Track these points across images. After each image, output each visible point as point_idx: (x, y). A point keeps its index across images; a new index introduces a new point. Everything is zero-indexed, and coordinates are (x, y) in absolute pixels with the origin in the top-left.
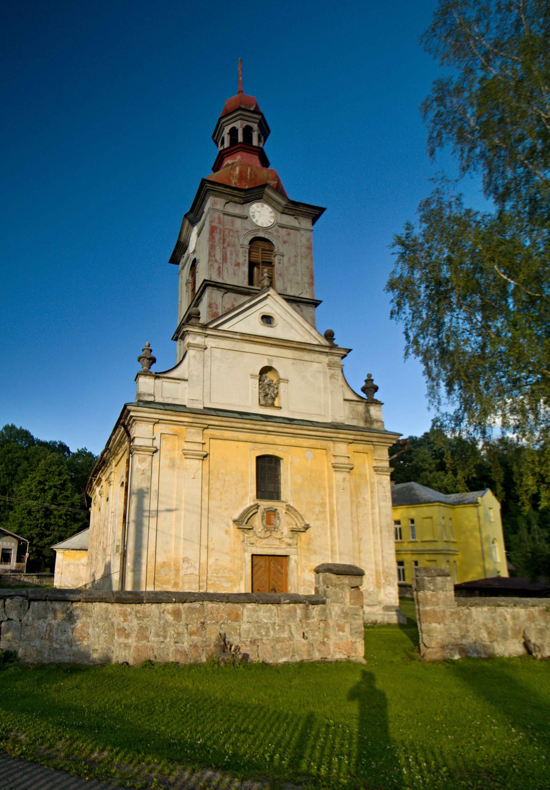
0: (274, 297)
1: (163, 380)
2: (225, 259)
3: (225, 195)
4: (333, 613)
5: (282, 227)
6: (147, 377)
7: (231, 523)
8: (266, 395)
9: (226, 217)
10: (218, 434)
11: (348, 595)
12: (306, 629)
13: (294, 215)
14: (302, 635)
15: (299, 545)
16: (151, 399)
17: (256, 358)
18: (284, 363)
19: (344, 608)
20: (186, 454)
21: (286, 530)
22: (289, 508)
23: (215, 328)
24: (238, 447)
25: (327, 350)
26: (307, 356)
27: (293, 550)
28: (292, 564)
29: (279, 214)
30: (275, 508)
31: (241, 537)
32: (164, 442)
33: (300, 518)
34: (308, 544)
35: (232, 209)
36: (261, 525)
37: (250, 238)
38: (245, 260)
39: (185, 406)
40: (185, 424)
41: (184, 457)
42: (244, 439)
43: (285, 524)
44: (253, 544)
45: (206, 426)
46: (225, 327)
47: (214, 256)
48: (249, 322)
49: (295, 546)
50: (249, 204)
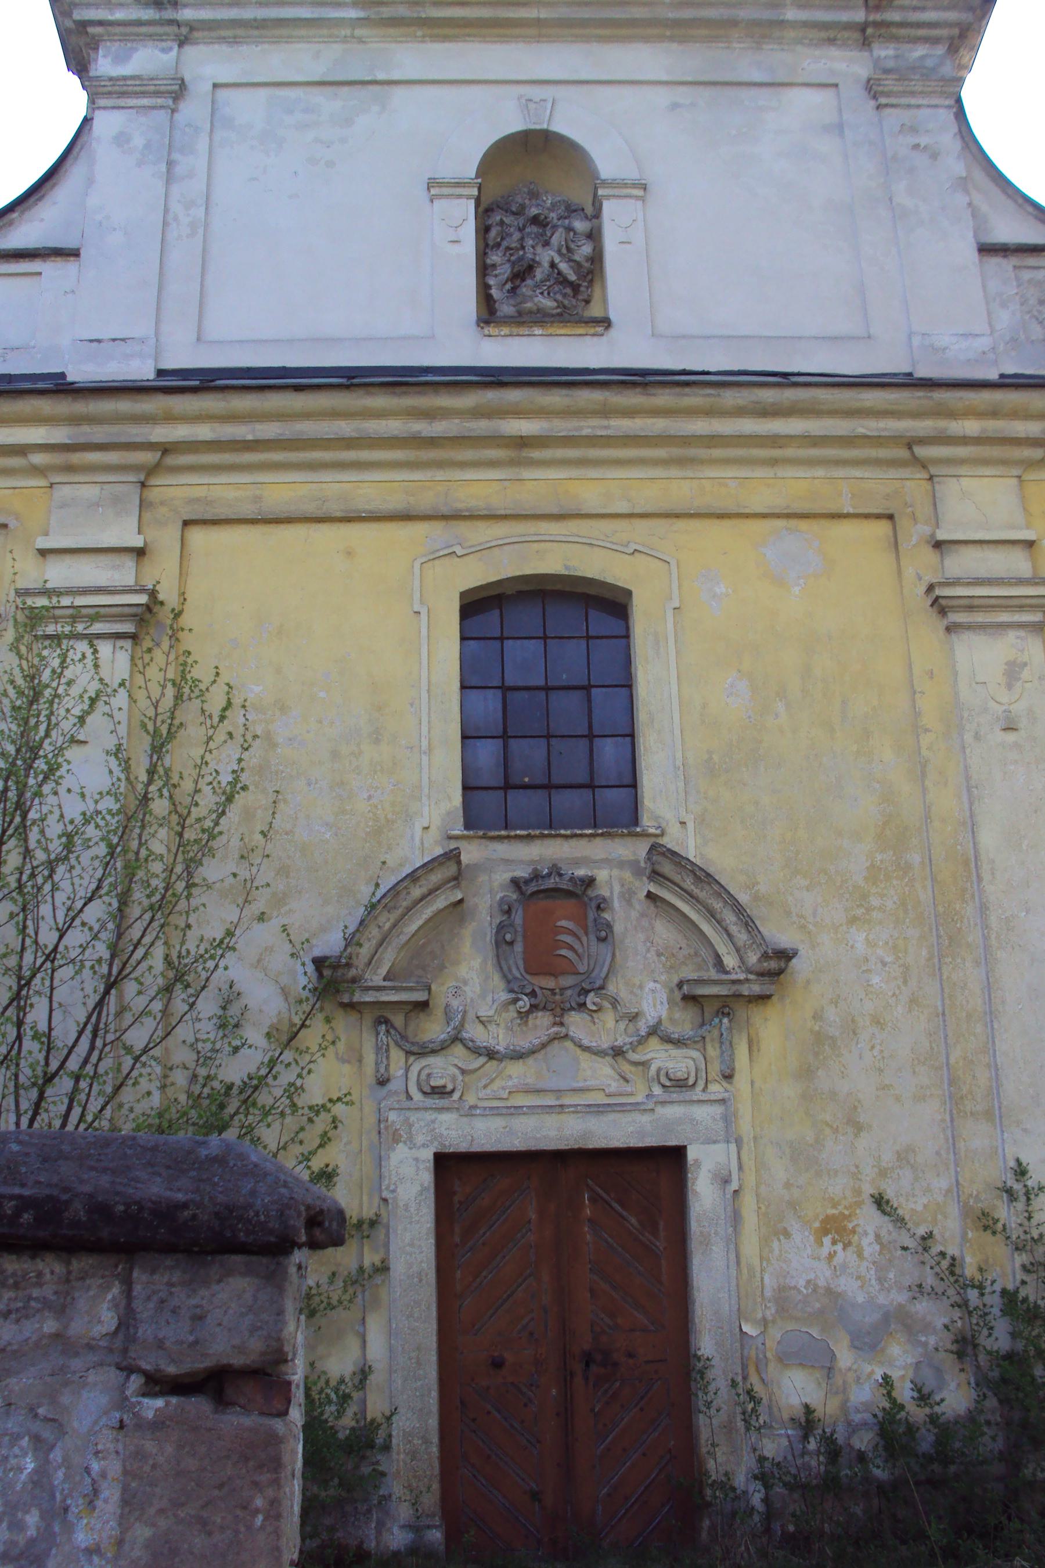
8: (522, 273)
10: (231, 494)
15: (742, 1080)
21: (654, 1002)
22: (664, 865)
24: (349, 553)
27: (704, 1113)
28: (703, 1194)
30: (581, 872)
33: (730, 918)
36: (497, 980)
40: (38, 459)
45: (148, 457)
49: (716, 1089)
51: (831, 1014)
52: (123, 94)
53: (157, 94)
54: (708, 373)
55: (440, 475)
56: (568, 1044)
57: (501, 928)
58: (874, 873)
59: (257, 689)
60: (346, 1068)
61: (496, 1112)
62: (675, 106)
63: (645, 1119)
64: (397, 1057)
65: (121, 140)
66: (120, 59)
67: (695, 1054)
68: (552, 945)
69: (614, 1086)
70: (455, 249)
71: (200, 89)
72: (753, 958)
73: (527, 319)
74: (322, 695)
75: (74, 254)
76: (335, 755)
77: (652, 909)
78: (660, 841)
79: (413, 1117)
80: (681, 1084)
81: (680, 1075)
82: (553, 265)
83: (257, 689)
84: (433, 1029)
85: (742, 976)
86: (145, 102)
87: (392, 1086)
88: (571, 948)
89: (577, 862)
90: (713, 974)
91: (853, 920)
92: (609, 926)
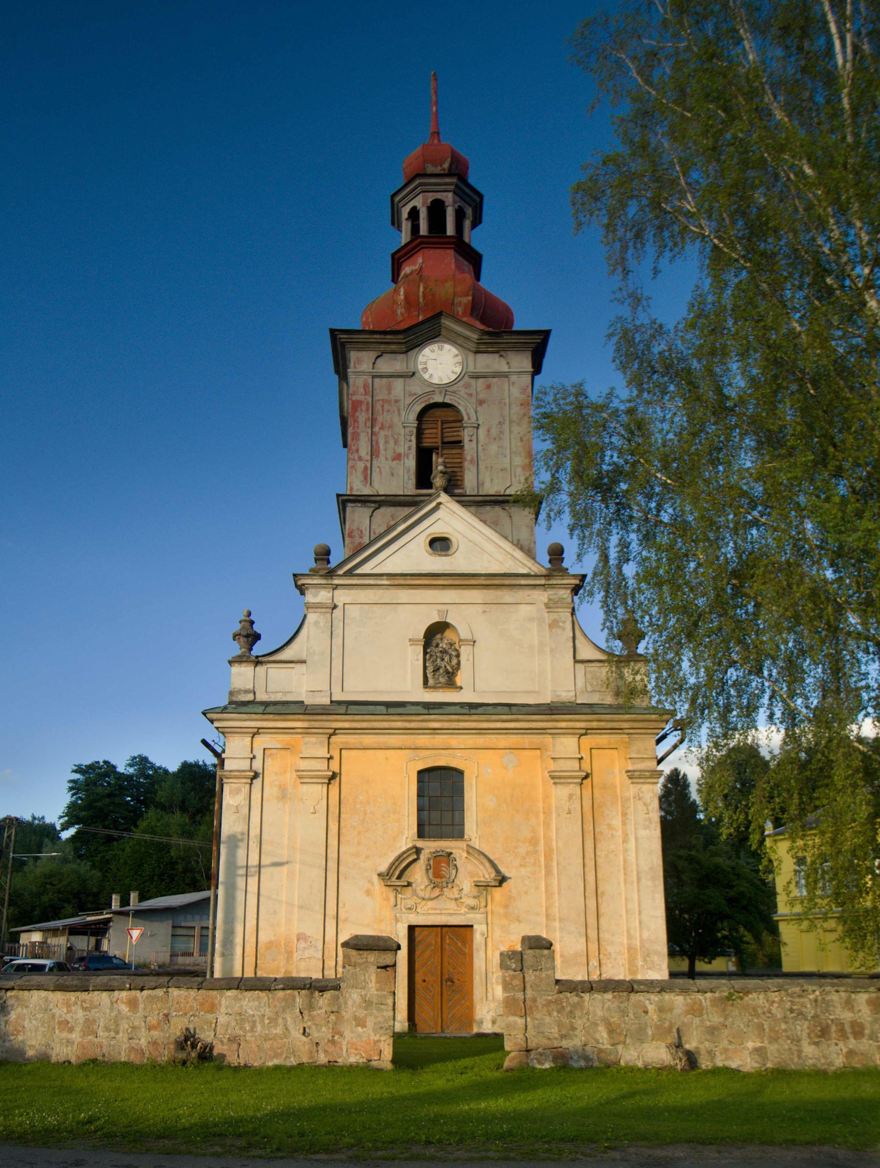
0: (448, 505)
1: (268, 665)
2: (374, 453)
3: (373, 346)
4: (350, 1002)
5: (476, 377)
6: (244, 665)
7: (375, 878)
10: (353, 741)
11: (373, 977)
13: (497, 352)
15: (489, 907)
17: (417, 612)
19: (366, 995)
20: (303, 777)
22: (471, 850)
23: (350, 573)
24: (387, 759)
28: (478, 938)
29: (471, 356)
30: (448, 850)
31: (392, 900)
32: (268, 762)
34: (506, 906)
37: (418, 408)
38: (410, 448)
39: (303, 702)
40: (299, 730)
41: (299, 781)
42: (397, 745)
44: (410, 909)
45: (331, 731)
46: (365, 569)
47: (357, 451)
48: (410, 554)
50: (417, 350)
51: (514, 891)
52: (316, 608)
53: (327, 608)
55: (412, 736)
58: (527, 853)
61: (424, 914)
62: (484, 612)
63: (463, 917)
65: (316, 623)
68: (441, 869)
70: (416, 662)
75: (304, 662)
76: (383, 817)
78: (469, 843)
80: (473, 908)
86: (323, 610)
89: (447, 848)
90: (482, 879)
91: (521, 866)
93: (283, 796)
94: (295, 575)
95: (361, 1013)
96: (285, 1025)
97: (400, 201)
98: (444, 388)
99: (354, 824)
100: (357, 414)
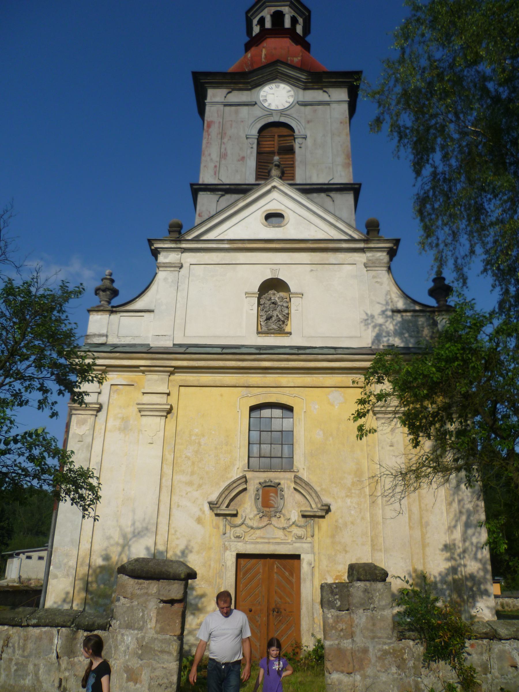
1: (122, 314)
4: (122, 648)
5: (305, 104)
6: (100, 313)
7: (206, 507)
8: (269, 318)
9: (227, 108)
11: (153, 614)
12: (67, 674)
14: (57, 684)
15: (316, 537)
16: (102, 340)
18: (293, 270)
19: (143, 637)
20: (143, 411)
21: (295, 516)
22: (298, 480)
23: (197, 240)
24: (222, 395)
25: (362, 245)
26: (331, 257)
27: (306, 546)
28: (305, 567)
29: (301, 92)
30: (277, 481)
31: (222, 528)
32: (114, 396)
33: (314, 495)
34: (333, 536)
35: (236, 97)
36: (254, 508)
37: (259, 125)
38: (251, 153)
41: (139, 414)
43: (293, 506)
44: (238, 537)
49: (309, 539)
50: (259, 88)
51: (340, 521)
52: (166, 267)
53: (175, 267)
54: (315, 348)
55: (245, 375)
56: (272, 526)
57: (256, 495)
58: (353, 484)
59: (197, 430)
60: (215, 530)
61: (252, 543)
62: (312, 270)
63: (291, 546)
64: (228, 527)
65: (165, 279)
66: (166, 257)
67: (304, 530)
69: (283, 537)
70: (252, 312)
71: (186, 266)
72: (319, 506)
73: (268, 332)
74: (213, 432)
77: (295, 492)
78: (297, 474)
79: (231, 543)
80: (300, 538)
81: (300, 535)
82: (277, 316)
83: (197, 430)
84: (238, 521)
85: (316, 510)
86: (172, 269)
87: (226, 535)
88: (273, 501)
89: (276, 479)
90: (309, 509)
91: (347, 496)
92: (283, 496)
93: (125, 427)
94: (149, 241)
95: (135, 663)
96: (36, 675)
97: (252, 15)
98: (282, 112)
99: (189, 454)
100: (210, 130)
